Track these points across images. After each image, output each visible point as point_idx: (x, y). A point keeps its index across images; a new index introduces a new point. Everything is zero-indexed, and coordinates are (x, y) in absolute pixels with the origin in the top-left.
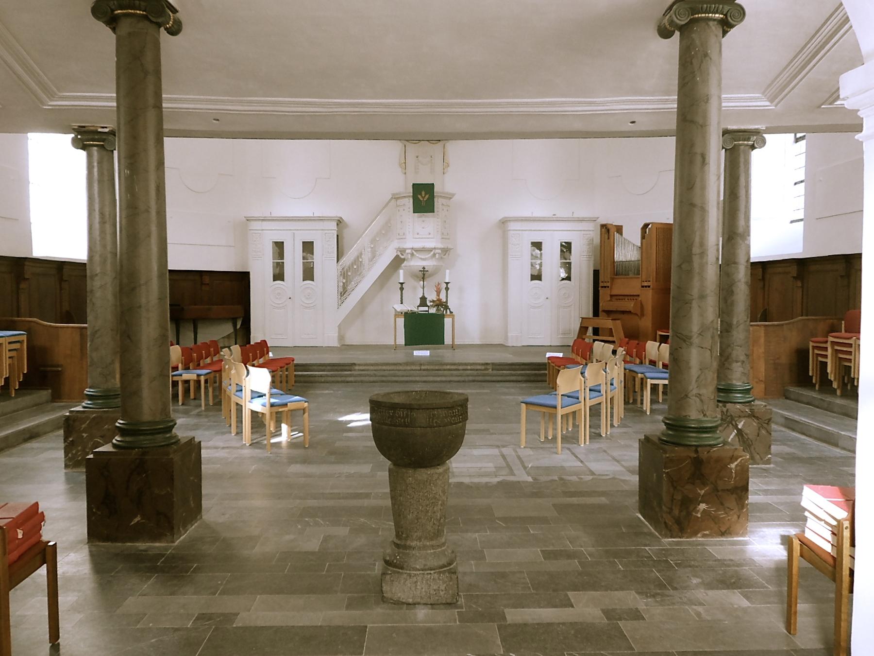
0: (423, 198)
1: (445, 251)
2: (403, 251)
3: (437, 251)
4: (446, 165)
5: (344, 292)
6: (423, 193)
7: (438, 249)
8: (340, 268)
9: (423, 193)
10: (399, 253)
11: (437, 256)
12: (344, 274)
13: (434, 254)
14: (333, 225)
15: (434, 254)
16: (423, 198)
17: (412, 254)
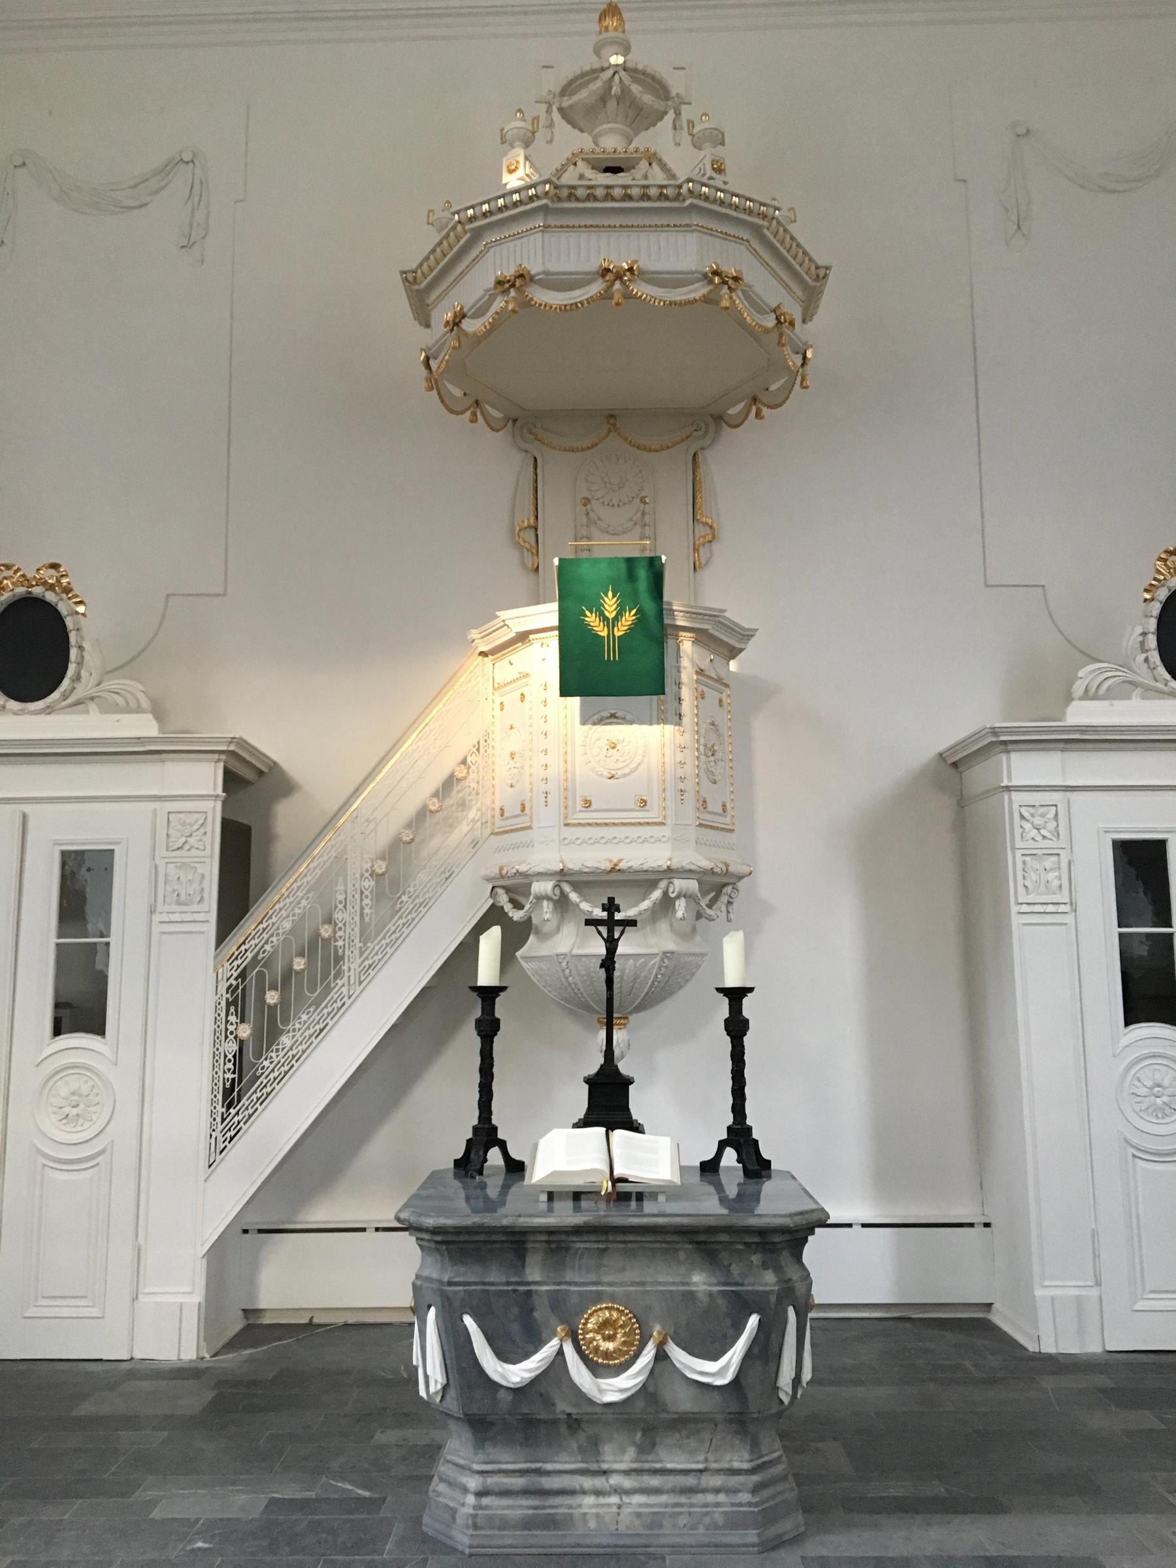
0: (611, 623)
1: (718, 886)
2: (516, 888)
3: (678, 884)
4: (704, 537)
5: (237, 1088)
6: (610, 604)
7: (686, 873)
8: (229, 972)
9: (610, 604)
10: (503, 899)
11: (681, 907)
12: (238, 1001)
13: (667, 903)
14: (207, 779)
15: (667, 903)
16: (611, 623)
17: (562, 904)
